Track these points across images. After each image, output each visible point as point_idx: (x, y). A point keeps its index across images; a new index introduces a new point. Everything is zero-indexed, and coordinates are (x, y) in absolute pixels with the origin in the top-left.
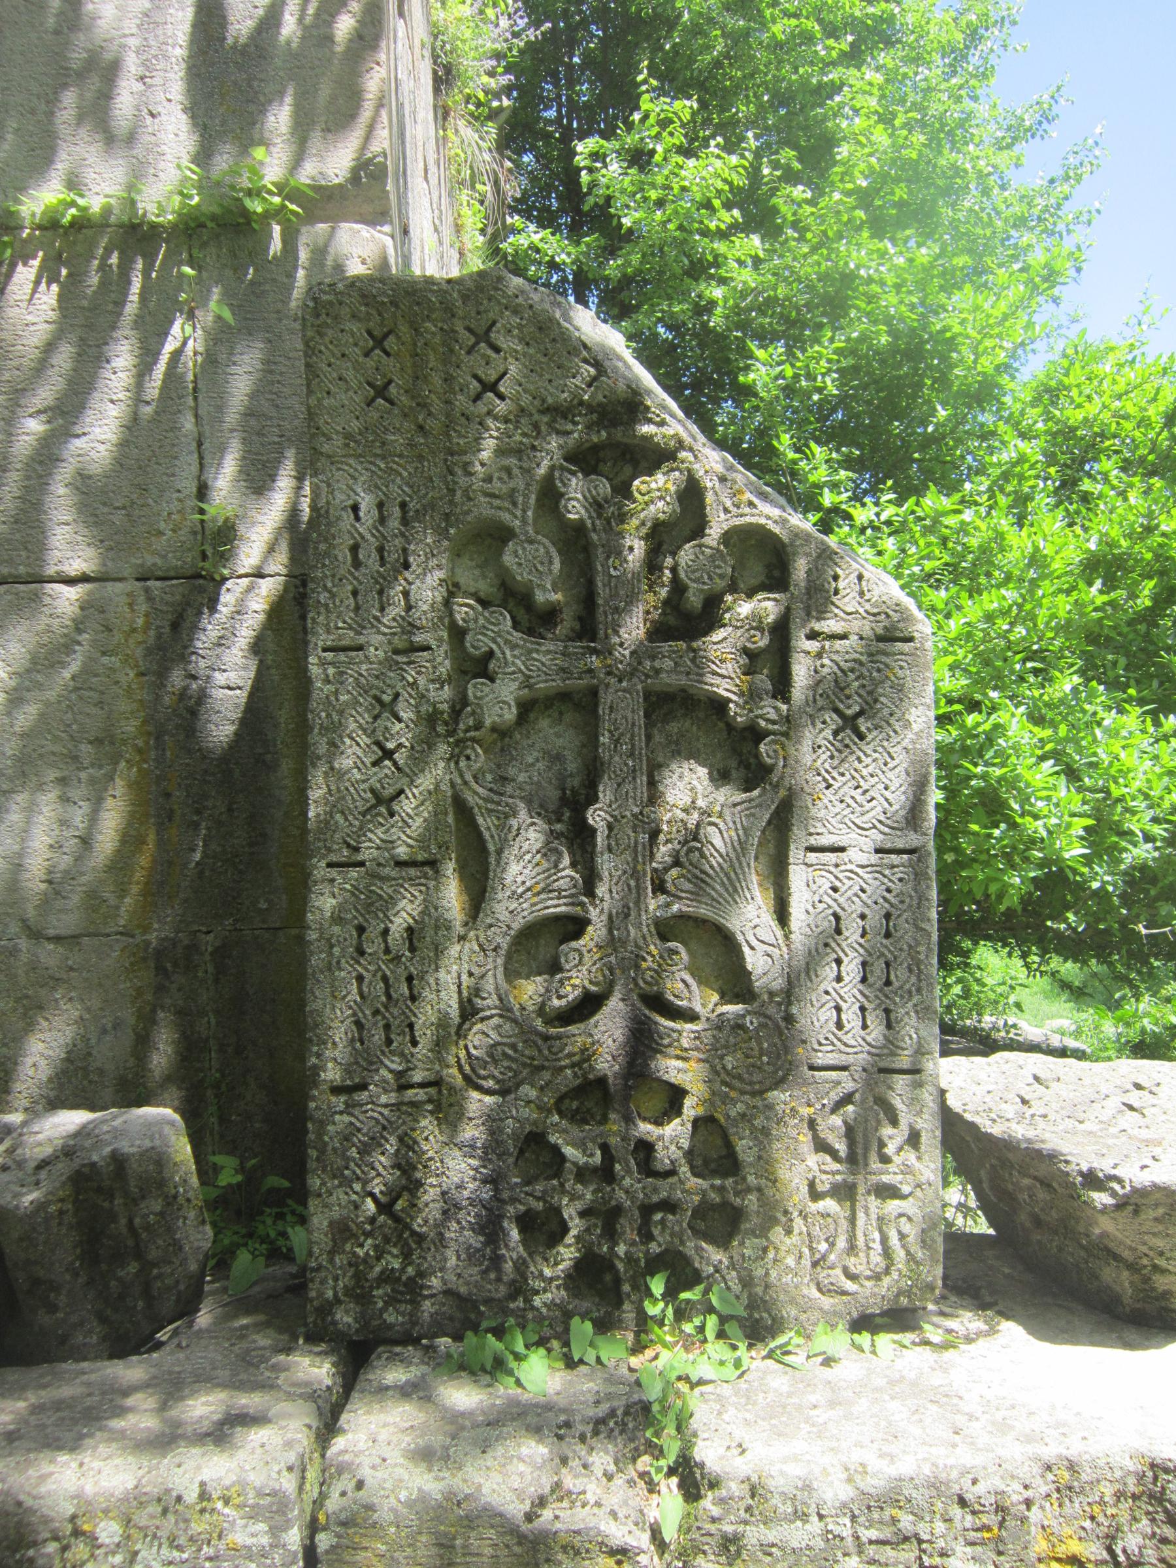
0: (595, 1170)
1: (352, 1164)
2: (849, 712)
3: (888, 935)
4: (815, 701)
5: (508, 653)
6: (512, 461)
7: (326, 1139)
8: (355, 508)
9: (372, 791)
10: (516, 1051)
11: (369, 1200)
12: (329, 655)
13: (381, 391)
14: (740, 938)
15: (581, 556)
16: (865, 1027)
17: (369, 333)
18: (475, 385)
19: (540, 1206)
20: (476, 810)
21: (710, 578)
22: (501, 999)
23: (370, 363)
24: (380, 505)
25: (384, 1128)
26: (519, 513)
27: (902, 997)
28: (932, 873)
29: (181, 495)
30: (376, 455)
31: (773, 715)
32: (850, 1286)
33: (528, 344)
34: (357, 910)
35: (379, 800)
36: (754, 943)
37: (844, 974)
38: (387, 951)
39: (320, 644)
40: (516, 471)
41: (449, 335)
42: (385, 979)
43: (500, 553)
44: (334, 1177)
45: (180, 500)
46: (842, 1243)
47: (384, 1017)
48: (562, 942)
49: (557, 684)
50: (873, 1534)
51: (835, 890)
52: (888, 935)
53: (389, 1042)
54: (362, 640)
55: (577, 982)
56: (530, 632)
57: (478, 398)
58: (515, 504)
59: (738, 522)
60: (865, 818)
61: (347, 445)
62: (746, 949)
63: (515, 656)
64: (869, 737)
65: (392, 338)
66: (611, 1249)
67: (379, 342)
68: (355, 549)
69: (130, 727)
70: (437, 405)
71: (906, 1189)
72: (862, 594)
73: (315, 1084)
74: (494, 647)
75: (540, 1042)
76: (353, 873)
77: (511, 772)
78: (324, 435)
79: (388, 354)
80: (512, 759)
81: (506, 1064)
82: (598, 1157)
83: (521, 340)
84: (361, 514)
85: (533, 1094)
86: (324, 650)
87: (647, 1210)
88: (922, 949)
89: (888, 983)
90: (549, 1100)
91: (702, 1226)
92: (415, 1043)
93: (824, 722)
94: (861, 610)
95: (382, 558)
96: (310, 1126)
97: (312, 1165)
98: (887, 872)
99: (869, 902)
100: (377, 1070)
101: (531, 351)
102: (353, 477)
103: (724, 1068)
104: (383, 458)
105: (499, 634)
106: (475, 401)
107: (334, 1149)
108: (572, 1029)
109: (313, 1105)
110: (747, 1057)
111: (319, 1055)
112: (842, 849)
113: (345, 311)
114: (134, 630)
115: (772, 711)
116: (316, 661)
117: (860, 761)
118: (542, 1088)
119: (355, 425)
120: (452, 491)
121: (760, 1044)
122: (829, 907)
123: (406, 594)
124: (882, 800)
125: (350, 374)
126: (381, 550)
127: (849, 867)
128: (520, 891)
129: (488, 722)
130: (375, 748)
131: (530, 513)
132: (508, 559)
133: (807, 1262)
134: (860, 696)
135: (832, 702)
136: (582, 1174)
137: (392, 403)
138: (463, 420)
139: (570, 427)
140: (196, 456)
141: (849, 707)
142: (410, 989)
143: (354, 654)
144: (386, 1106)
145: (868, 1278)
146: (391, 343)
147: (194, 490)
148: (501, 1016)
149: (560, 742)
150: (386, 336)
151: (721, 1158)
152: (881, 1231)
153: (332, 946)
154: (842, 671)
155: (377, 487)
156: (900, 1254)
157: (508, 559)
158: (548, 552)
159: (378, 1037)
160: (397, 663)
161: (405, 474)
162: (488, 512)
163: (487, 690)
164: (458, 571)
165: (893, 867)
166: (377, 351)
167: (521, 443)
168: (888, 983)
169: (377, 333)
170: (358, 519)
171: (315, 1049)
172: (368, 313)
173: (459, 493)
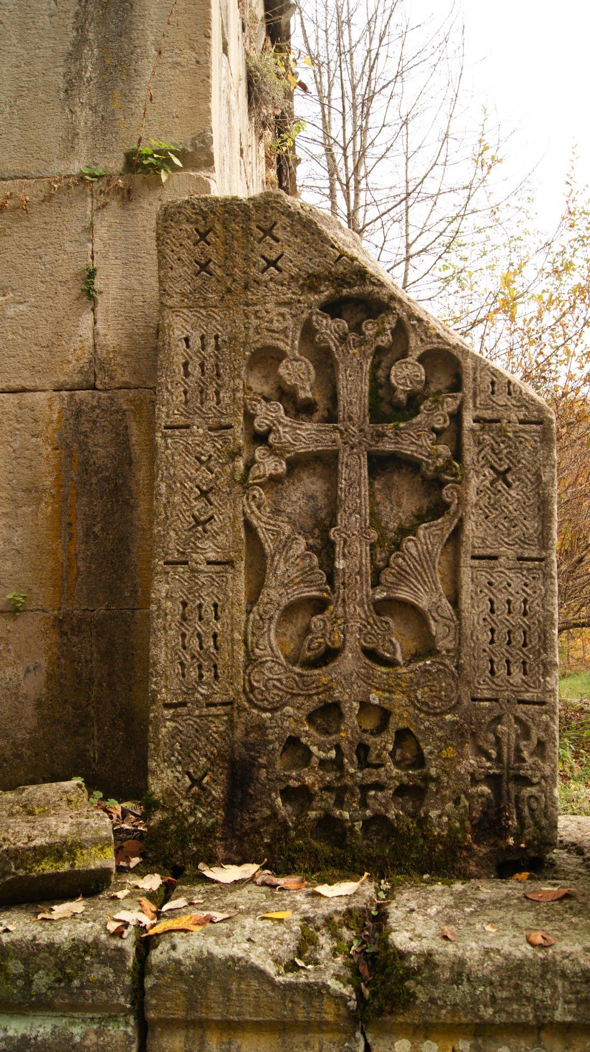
0: (331, 761)
1: (176, 754)
2: (502, 469)
3: (525, 614)
8: (187, 340)
9: (194, 516)
10: (282, 684)
12: (169, 432)
13: (204, 267)
16: (509, 673)
17: (197, 230)
20: (259, 530)
21: (411, 383)
23: (197, 250)
24: (202, 338)
25: (197, 731)
26: (290, 342)
27: (534, 654)
28: (555, 574)
30: (201, 307)
33: (296, 236)
34: (183, 592)
35: (198, 523)
36: (438, 618)
38: (201, 618)
39: (163, 424)
40: (288, 316)
41: (247, 232)
42: (199, 636)
43: (277, 367)
44: (165, 761)
45: (80, 341)
47: (198, 660)
48: (312, 616)
50: (505, 994)
52: (525, 614)
53: (201, 676)
54: (189, 422)
56: (296, 417)
57: (263, 271)
58: (287, 337)
59: (429, 347)
62: (432, 622)
63: (285, 432)
64: (514, 485)
65: (211, 234)
67: (203, 236)
68: (186, 365)
69: (48, 482)
71: (535, 780)
73: (154, 702)
75: (297, 678)
78: (169, 295)
79: (209, 244)
81: (275, 692)
83: (292, 234)
86: (166, 428)
87: (365, 788)
93: (484, 475)
94: (509, 404)
95: (203, 371)
96: (150, 728)
98: (525, 573)
100: (193, 694)
101: (298, 241)
102: (186, 320)
103: (416, 698)
104: (205, 308)
106: (262, 273)
107: (165, 744)
110: (431, 691)
111: (156, 683)
112: (495, 558)
114: (52, 422)
116: (160, 434)
117: (508, 501)
119: (188, 288)
120: (247, 328)
122: (487, 595)
123: (217, 393)
124: (521, 525)
125: (184, 257)
126: (202, 365)
127: (500, 569)
130: (196, 490)
131: (296, 342)
132: (282, 371)
134: (508, 458)
136: (323, 763)
138: (255, 285)
141: (501, 466)
142: (215, 642)
143: (184, 430)
144: (198, 717)
146: (211, 237)
148: (273, 661)
149: (314, 487)
150: (207, 232)
152: (517, 807)
153: (166, 614)
155: (200, 326)
156: (529, 821)
157: (282, 371)
158: (307, 367)
159: (194, 674)
160: (211, 436)
161: (219, 318)
162: (269, 342)
164: (251, 380)
166: (202, 242)
167: (291, 298)
169: (202, 231)
170: (188, 346)
171: (154, 679)
172: (197, 219)
173: (252, 330)
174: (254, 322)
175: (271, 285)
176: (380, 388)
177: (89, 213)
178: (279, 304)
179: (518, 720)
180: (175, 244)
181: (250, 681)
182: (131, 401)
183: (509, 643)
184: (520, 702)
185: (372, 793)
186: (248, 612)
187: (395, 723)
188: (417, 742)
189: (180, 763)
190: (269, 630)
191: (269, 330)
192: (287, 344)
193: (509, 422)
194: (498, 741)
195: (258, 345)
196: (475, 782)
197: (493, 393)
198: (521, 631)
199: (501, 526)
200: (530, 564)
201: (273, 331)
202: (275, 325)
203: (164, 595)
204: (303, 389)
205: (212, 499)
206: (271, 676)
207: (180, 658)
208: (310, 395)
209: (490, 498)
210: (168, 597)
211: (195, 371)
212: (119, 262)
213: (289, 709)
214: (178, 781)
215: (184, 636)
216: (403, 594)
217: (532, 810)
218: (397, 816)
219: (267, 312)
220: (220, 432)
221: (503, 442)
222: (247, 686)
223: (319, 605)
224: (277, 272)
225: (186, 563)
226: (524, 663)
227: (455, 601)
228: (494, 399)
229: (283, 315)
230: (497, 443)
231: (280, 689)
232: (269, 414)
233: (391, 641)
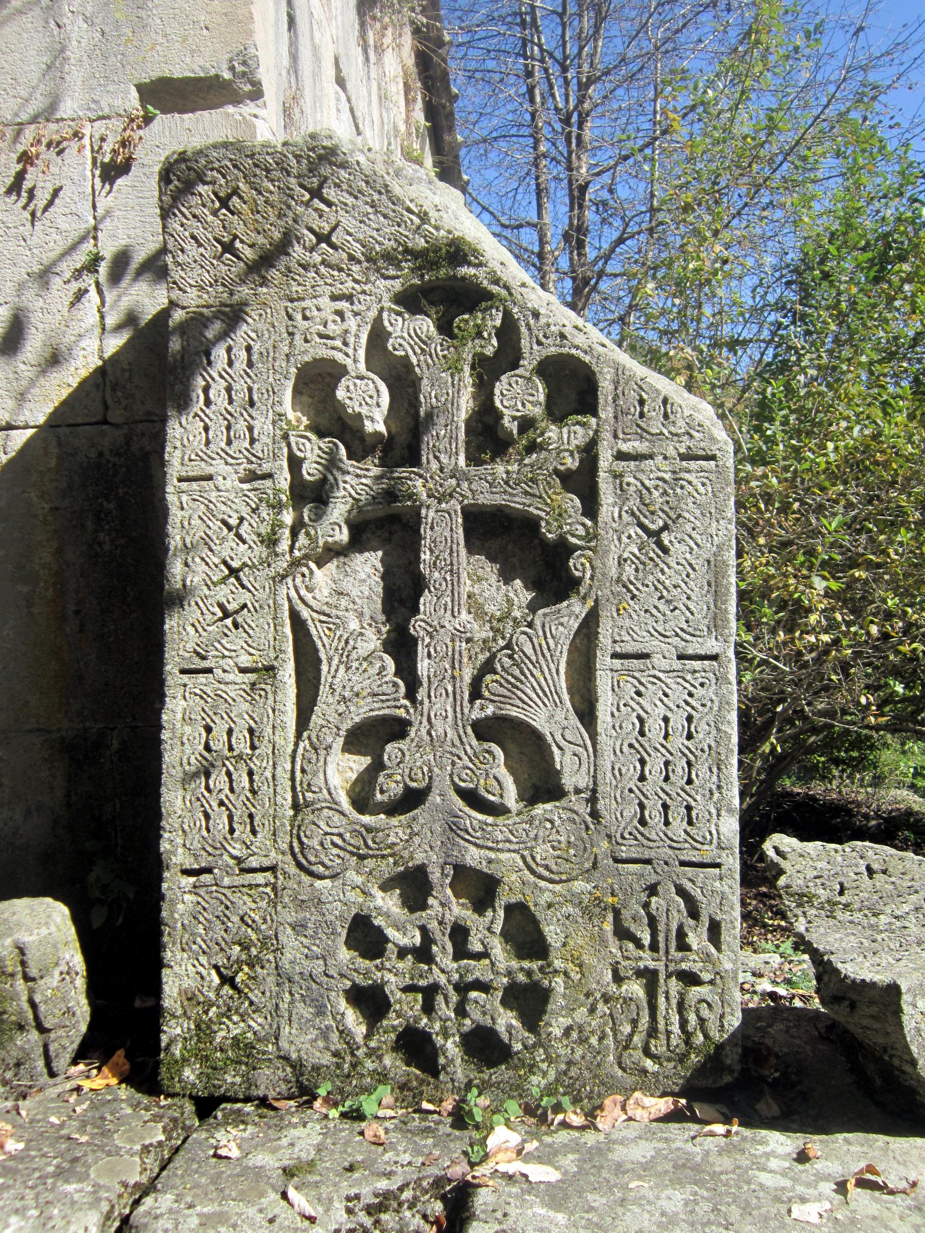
1: (199, 940)
3: (689, 737)
4: (620, 516)
6: (343, 305)
11: (213, 972)
12: (184, 485)
14: (549, 739)
16: (667, 823)
20: (310, 622)
21: (523, 405)
32: (649, 1064)
36: (562, 743)
39: (175, 474)
40: (348, 314)
51: (639, 694)
53: (232, 831)
54: (210, 470)
55: (399, 778)
57: (312, 250)
58: (346, 344)
62: (555, 749)
65: (235, 199)
67: (224, 202)
71: (706, 976)
72: (666, 416)
76: (202, 678)
79: (233, 213)
81: (335, 851)
82: (418, 940)
86: (180, 480)
87: (463, 988)
88: (722, 750)
89: (690, 782)
92: (254, 832)
93: (629, 537)
94: (665, 432)
108: (395, 821)
112: (646, 656)
115: (580, 527)
123: (250, 429)
126: (229, 389)
127: (652, 672)
130: (223, 567)
135: (638, 519)
136: (402, 953)
142: (251, 781)
143: (204, 483)
145: (669, 1060)
148: (330, 808)
150: (229, 197)
154: (648, 489)
168: (690, 782)
169: (222, 195)
178: (334, 298)
179: (681, 891)
183: (667, 779)
184: (683, 864)
185: (473, 994)
187: (504, 898)
191: (321, 336)
192: (347, 355)
193: (665, 458)
194: (653, 922)
195: (307, 358)
197: (642, 415)
200: (697, 665)
201: (328, 337)
206: (329, 830)
209: (637, 570)
217: (702, 1021)
218: (510, 1028)
222: (296, 844)
225: (209, 671)
226: (689, 808)
228: (643, 425)
230: (648, 489)
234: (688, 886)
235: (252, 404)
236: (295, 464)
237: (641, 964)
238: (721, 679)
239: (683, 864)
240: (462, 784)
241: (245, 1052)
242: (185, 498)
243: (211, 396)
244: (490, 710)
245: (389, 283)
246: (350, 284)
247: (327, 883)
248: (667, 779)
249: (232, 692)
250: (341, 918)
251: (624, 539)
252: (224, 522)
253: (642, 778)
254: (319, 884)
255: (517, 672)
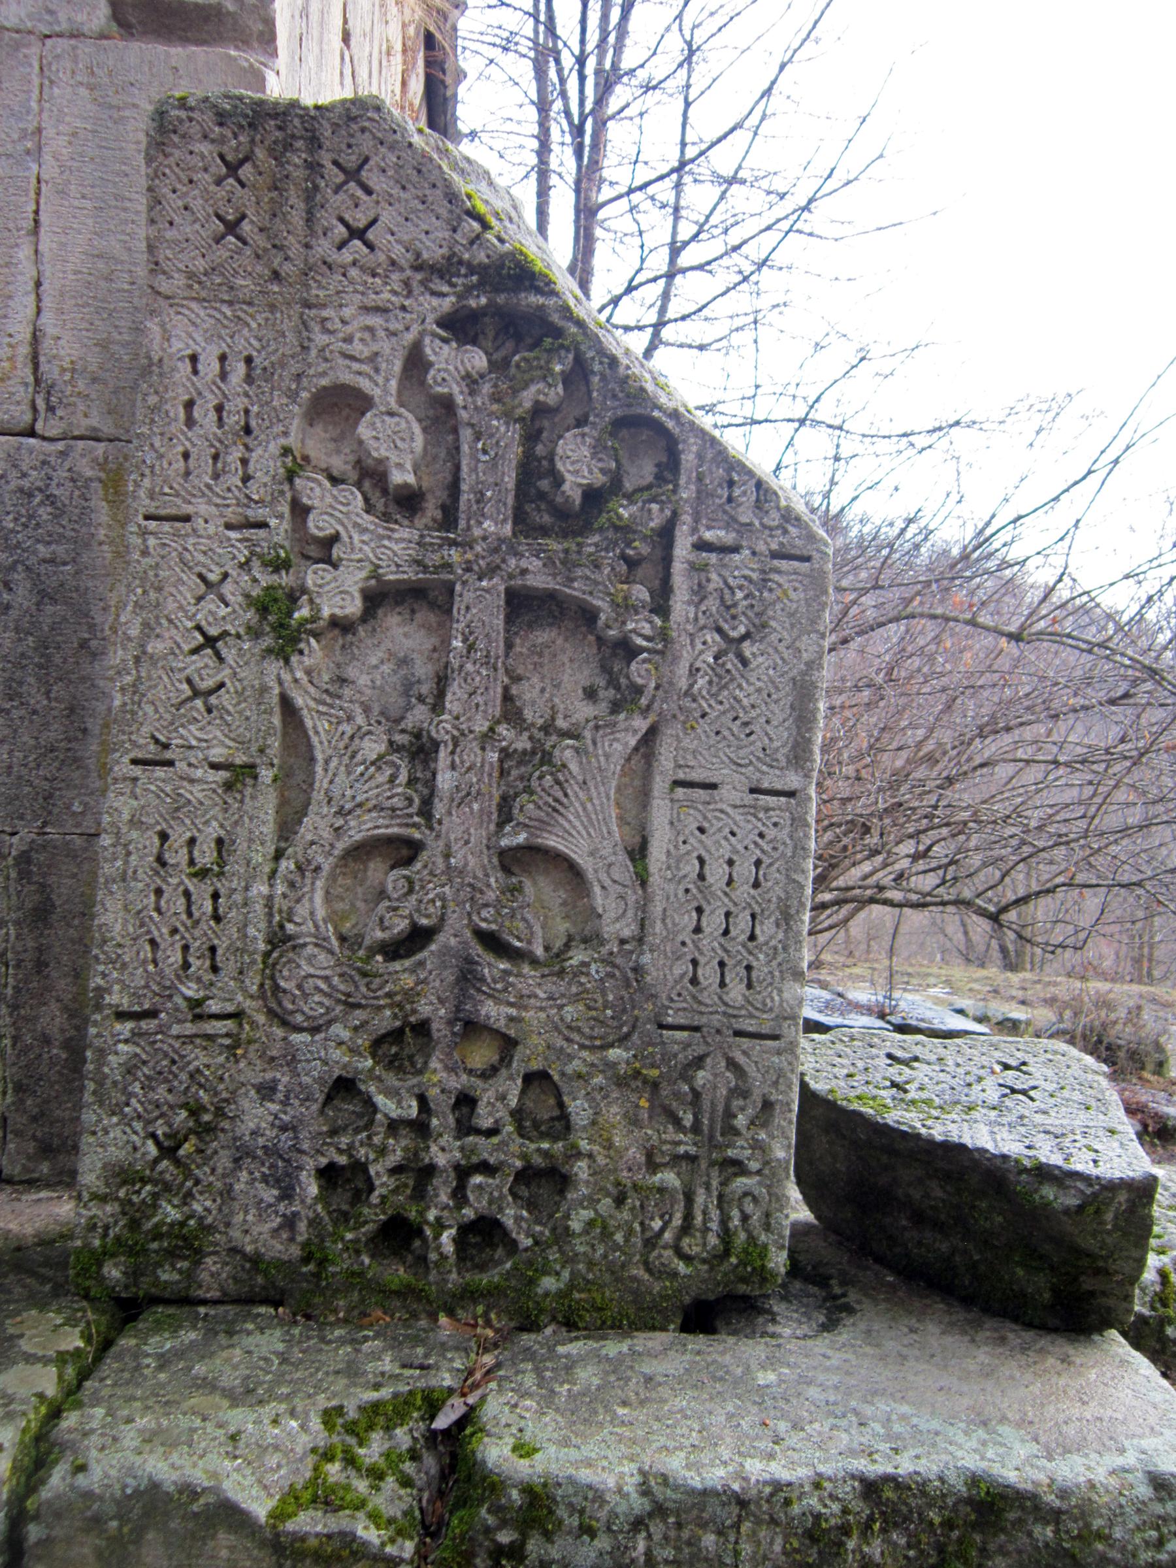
1: (133, 1101)
2: (734, 634)
3: (756, 885)
4: (696, 619)
5: (356, 537)
6: (375, 321)
7: (106, 1070)
8: (194, 359)
11: (150, 1142)
12: (152, 525)
13: (232, 227)
14: (590, 875)
15: (450, 438)
16: (722, 984)
17: (222, 157)
18: (341, 230)
19: (343, 1160)
20: (305, 712)
22: (316, 927)
24: (223, 358)
28: (811, 819)
29: (13, 341)
31: (647, 629)
32: (681, 1268)
35: (196, 693)
37: (704, 923)
39: (142, 510)
41: (314, 167)
42: (187, 894)
44: (114, 1114)
45: (10, 345)
46: (677, 1221)
48: (393, 867)
49: (410, 574)
51: (702, 830)
53: (186, 965)
54: (188, 509)
56: (386, 517)
58: (377, 370)
60: (742, 753)
61: (190, 287)
62: (597, 889)
66: (421, 1213)
67: (233, 169)
68: (189, 405)
70: (295, 249)
71: (754, 1165)
74: (340, 529)
76: (160, 772)
77: (351, 672)
79: (243, 185)
80: (354, 658)
81: (317, 998)
82: (414, 1112)
84: (200, 367)
85: (345, 1035)
89: (752, 937)
90: (363, 1041)
91: (524, 1192)
95: (220, 419)
96: (89, 1054)
97: (88, 1097)
99: (740, 847)
100: (170, 996)
104: (230, 303)
105: (347, 514)
106: (340, 248)
107: (115, 1083)
109: (93, 1031)
110: (589, 1008)
111: (104, 975)
113: (195, 130)
116: (134, 529)
118: (356, 1029)
119: (201, 264)
121: (604, 994)
123: (244, 462)
125: (197, 204)
126: (219, 409)
128: (348, 806)
129: (326, 612)
133: (637, 1241)
136: (393, 1126)
137: (245, 243)
138: (325, 268)
139: (445, 289)
140: (33, 297)
141: (734, 628)
143: (178, 525)
144: (178, 1037)
145: (704, 1261)
146: (246, 171)
147: (29, 336)
150: (242, 163)
151: (552, 1119)
154: (730, 588)
155: (220, 337)
157: (364, 431)
161: (254, 325)
162: (346, 378)
163: (329, 577)
164: (310, 443)
165: (767, 810)
168: (752, 937)
169: (229, 158)
170: (195, 372)
172: (223, 136)
173: (314, 353)
174: (320, 339)
175: (354, 272)
176: (536, 473)
177: (34, 105)
178: (366, 309)
180: (180, 180)
181: (273, 978)
182: (102, 466)
183: (726, 932)
184: (738, 1033)
185: (478, 1179)
186: (278, 855)
188: (558, 1095)
189: (139, 1117)
190: (313, 890)
195: (324, 382)
196: (652, 1166)
197: (730, 500)
198: (748, 912)
199: (726, 733)
200: (771, 800)
201: (352, 358)
202: (357, 348)
203: (126, 816)
204: (400, 466)
205: (224, 652)
206: (312, 971)
207: (149, 932)
208: (411, 479)
210: (135, 823)
211: (205, 415)
212: (88, 204)
213: (339, 1031)
214: (135, 1149)
215: (159, 892)
216: (552, 842)
219: (344, 322)
220: (247, 533)
221: (741, 588)
223: (405, 851)
224: (366, 250)
225: (170, 763)
226: (749, 968)
227: (638, 853)
229: (370, 329)
231: (326, 994)
232: (337, 509)
233: (524, 919)
234: (741, 1059)
235: (248, 430)
236: (300, 511)
237: (682, 1149)
238: (799, 822)
239: (738, 1033)
240: (484, 925)
241: (188, 1243)
242: (152, 542)
243: (196, 414)
244: (521, 838)
245: (435, 302)
246: (386, 295)
247: (304, 1037)
248: (726, 932)
249: (196, 793)
250: (320, 1080)
251: (700, 647)
252: (201, 576)
253: (698, 930)
254: (297, 1038)
255: (560, 795)
